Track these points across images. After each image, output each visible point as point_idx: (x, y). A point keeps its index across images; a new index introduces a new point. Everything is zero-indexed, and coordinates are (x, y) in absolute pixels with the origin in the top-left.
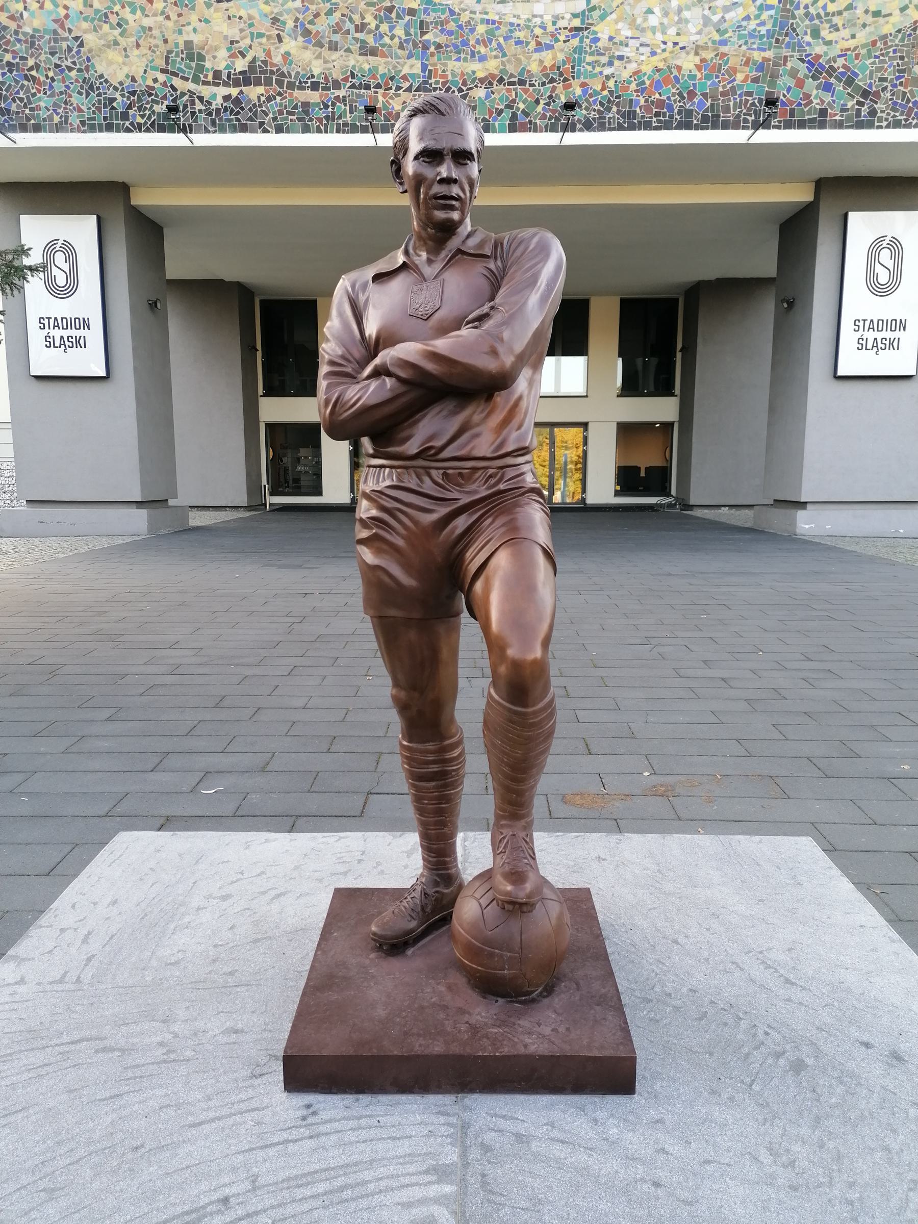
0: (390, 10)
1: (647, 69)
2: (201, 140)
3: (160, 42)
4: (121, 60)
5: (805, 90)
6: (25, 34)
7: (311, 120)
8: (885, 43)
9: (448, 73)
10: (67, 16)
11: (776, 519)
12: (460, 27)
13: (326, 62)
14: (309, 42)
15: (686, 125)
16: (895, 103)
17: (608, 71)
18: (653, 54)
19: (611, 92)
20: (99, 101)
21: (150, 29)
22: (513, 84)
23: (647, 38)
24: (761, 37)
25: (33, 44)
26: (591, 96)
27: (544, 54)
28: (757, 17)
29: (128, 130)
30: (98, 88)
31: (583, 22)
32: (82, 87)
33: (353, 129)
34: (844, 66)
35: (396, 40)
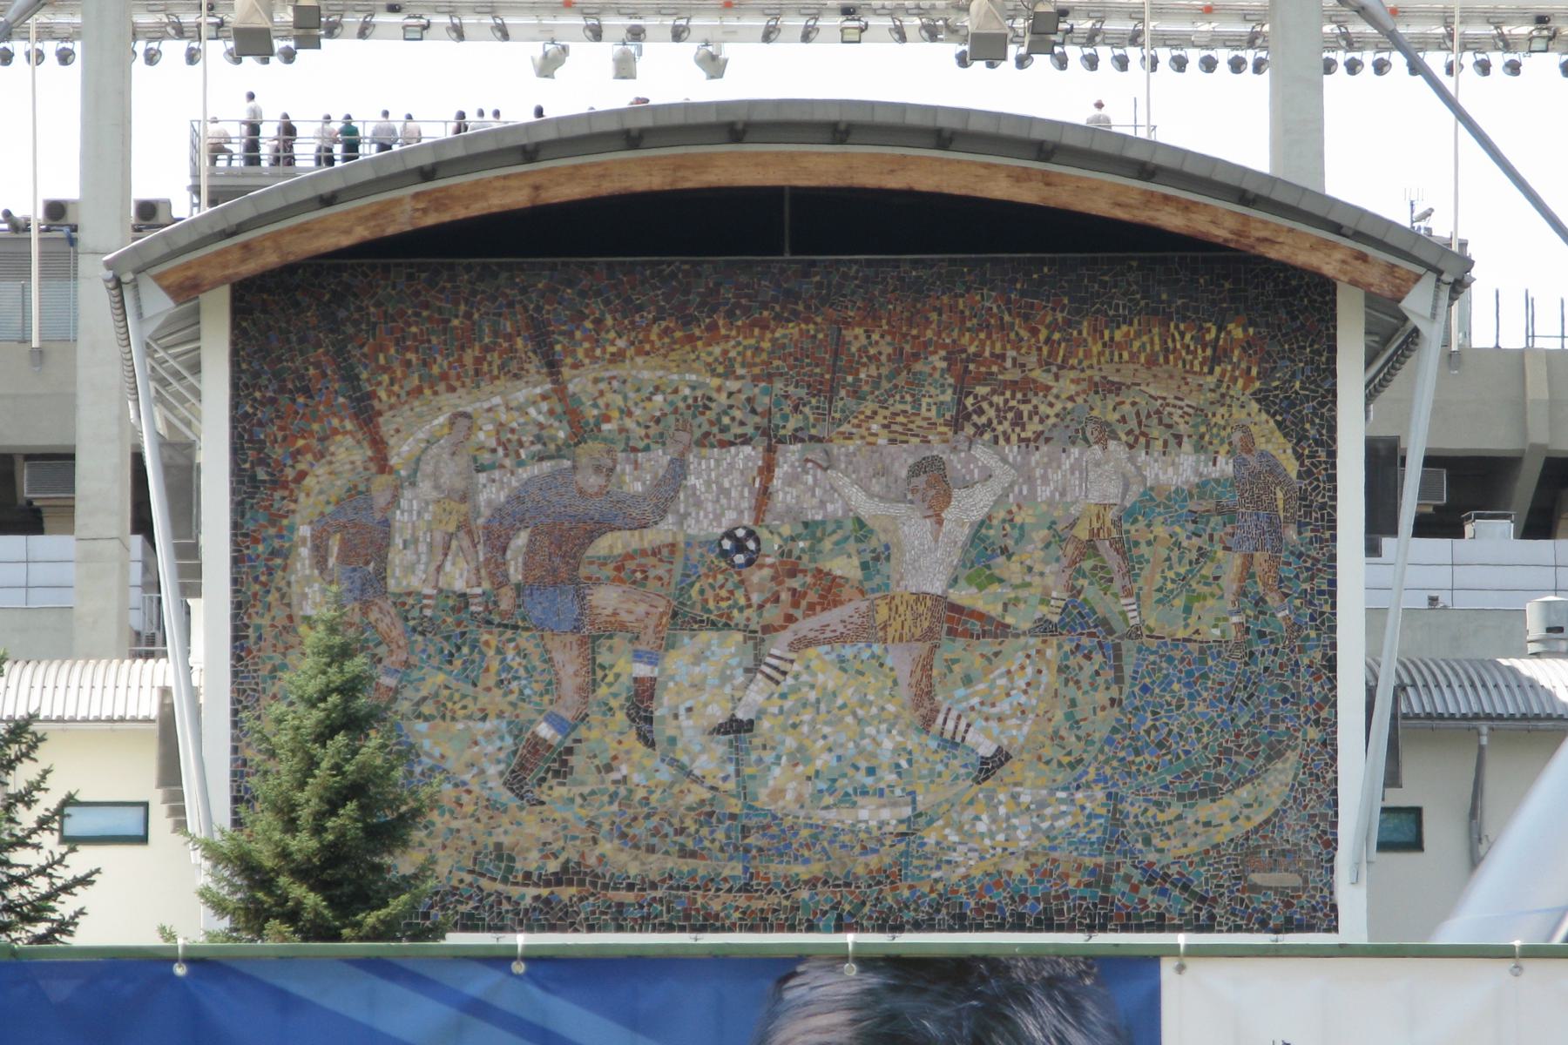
1: (978, 874)
3: (468, 844)
12: (783, 831)
13: (643, 864)
19: (940, 895)
21: (458, 831)
28: (1087, 825)
33: (670, 928)
35: (717, 844)
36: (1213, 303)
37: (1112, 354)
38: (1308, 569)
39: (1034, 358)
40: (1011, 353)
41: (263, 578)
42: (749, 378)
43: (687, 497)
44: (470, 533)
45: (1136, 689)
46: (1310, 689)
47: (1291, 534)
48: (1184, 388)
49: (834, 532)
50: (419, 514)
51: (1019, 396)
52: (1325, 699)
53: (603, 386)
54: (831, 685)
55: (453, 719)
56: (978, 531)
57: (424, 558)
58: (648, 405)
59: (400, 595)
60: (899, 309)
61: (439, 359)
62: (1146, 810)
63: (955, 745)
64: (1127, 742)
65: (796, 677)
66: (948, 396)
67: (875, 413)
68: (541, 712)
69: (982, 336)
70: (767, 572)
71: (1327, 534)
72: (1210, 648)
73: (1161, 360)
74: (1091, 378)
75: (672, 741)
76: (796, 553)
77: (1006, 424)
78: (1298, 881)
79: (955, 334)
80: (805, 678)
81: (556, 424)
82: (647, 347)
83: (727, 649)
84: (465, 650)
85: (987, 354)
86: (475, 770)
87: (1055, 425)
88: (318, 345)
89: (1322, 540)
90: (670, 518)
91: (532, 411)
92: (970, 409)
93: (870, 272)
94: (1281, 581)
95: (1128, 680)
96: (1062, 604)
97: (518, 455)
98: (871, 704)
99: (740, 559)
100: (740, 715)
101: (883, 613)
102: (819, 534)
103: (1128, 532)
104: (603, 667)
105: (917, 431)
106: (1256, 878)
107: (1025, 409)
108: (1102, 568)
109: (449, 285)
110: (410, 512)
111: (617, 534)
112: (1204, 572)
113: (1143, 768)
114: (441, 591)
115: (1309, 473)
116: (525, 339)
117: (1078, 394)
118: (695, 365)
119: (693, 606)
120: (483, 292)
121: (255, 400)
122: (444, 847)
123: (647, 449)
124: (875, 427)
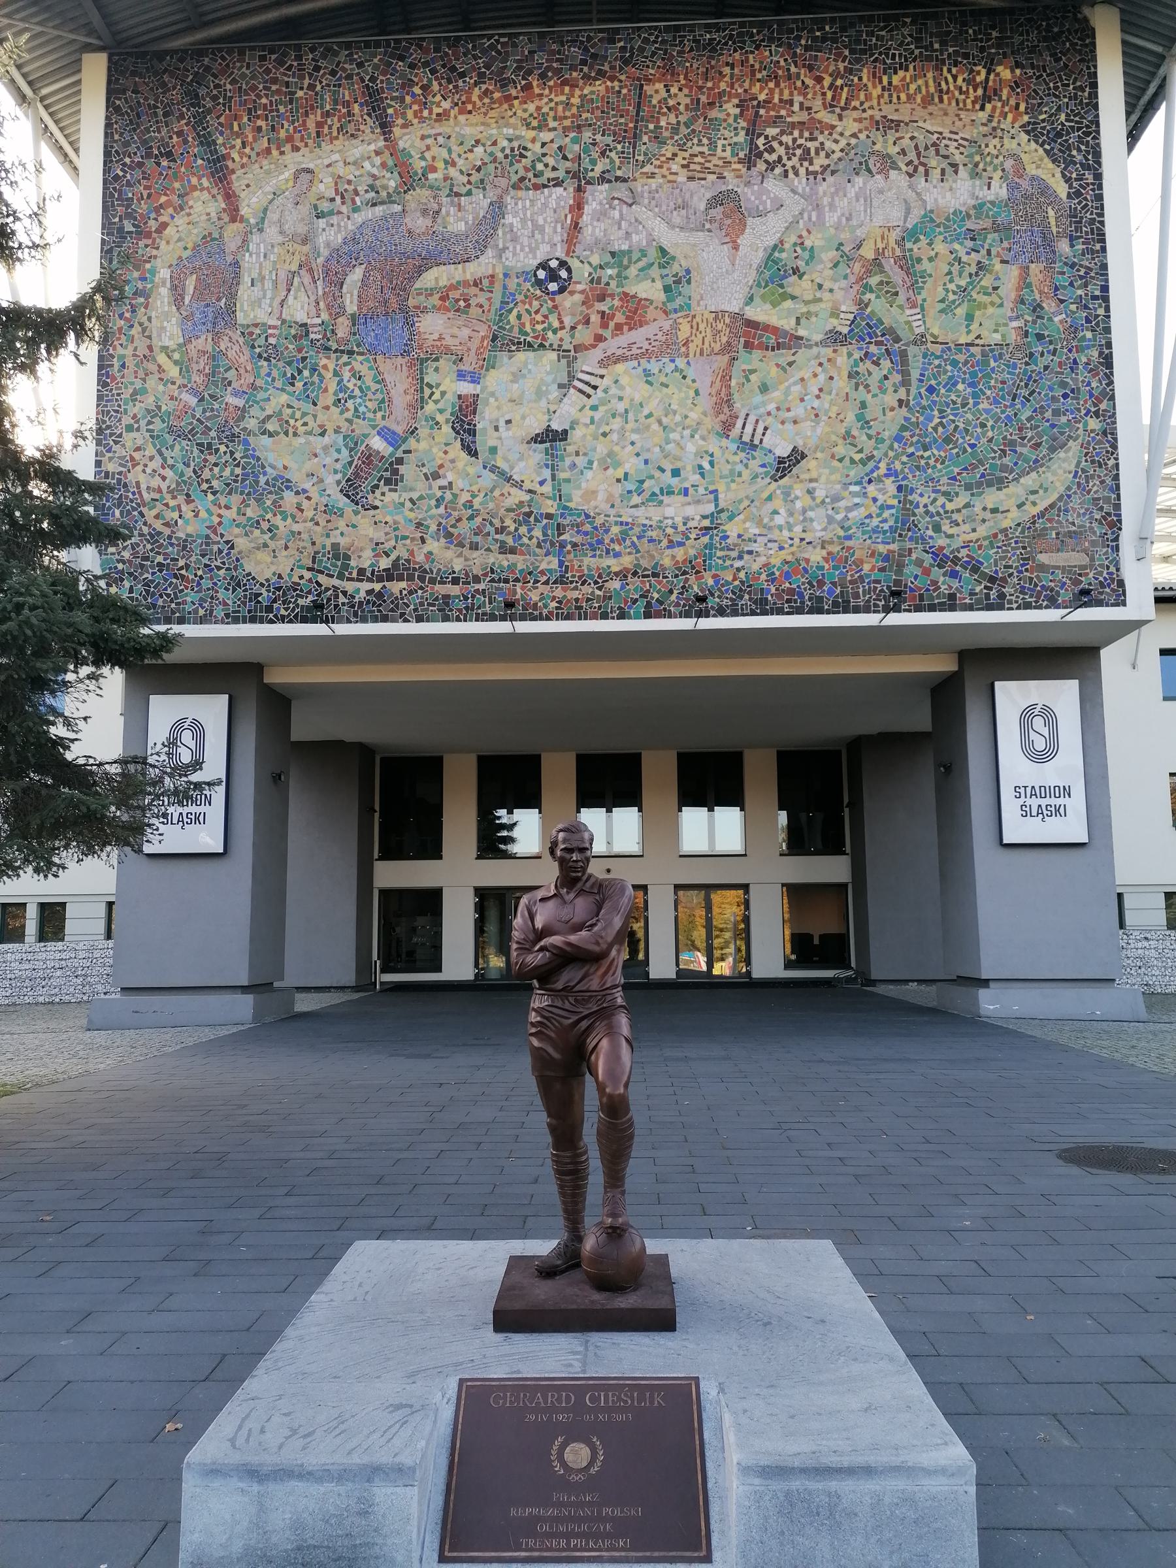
0: (529, 514)
1: (776, 561)
2: (342, 629)
4: (269, 559)
5: (932, 577)
6: (178, 539)
7: (451, 610)
8: (1006, 535)
9: (585, 568)
10: (220, 523)
11: (956, 997)
12: (596, 528)
13: (466, 560)
14: (451, 543)
15: (819, 611)
16: (1023, 587)
17: (738, 564)
18: (781, 548)
19: (742, 582)
20: (245, 596)
21: (299, 533)
22: (648, 576)
23: (775, 535)
24: (885, 532)
25: (185, 547)
26: (723, 585)
27: (676, 549)
28: (878, 515)
29: (271, 622)
30: (245, 585)
31: (712, 523)
32: (229, 584)
33: (493, 618)
34: (968, 556)
35: (535, 540)
36: (982, 49)
37: (890, 96)
38: (1081, 277)
39: (817, 104)
40: (798, 99)
41: (127, 315)
42: (560, 131)
43: (504, 233)
44: (311, 271)
45: (923, 391)
46: (1089, 384)
47: (1064, 246)
48: (958, 123)
49: (639, 260)
50: (265, 256)
51: (806, 134)
52: (1104, 393)
53: (429, 141)
54: (638, 398)
55: (295, 434)
56: (771, 255)
57: (269, 294)
58: (469, 155)
59: (248, 326)
60: (695, 66)
61: (286, 126)
62: (935, 500)
63: (754, 447)
64: (915, 439)
65: (606, 391)
66: (741, 137)
67: (675, 155)
68: (374, 427)
69: (771, 85)
70: (578, 298)
71: (1098, 246)
72: (992, 351)
73: (936, 100)
74: (872, 117)
75: (493, 450)
76: (604, 281)
77: (795, 160)
78: (1086, 560)
79: (746, 85)
80: (614, 391)
81: (388, 175)
82: (470, 107)
83: (543, 367)
84: (306, 373)
85: (776, 100)
86: (315, 479)
87: (840, 159)
88: (182, 116)
89: (1093, 252)
90: (490, 252)
91: (367, 165)
92: (762, 148)
93: (668, 37)
94: (1056, 289)
95: (914, 383)
96: (851, 317)
97: (354, 202)
98: (675, 413)
99: (553, 287)
100: (555, 426)
101: (685, 331)
102: (625, 262)
103: (911, 250)
104: (430, 386)
105: (713, 169)
106: (1043, 558)
107: (812, 145)
108: (888, 283)
109: (295, 64)
110: (258, 254)
111: (442, 268)
112: (983, 283)
113: (932, 462)
114: (284, 322)
115: (1078, 194)
116: (361, 105)
117: (860, 131)
118: (512, 120)
119: (511, 330)
120: (326, 68)
121: (124, 165)
122: (286, 548)
123: (469, 193)
124: (675, 167)
